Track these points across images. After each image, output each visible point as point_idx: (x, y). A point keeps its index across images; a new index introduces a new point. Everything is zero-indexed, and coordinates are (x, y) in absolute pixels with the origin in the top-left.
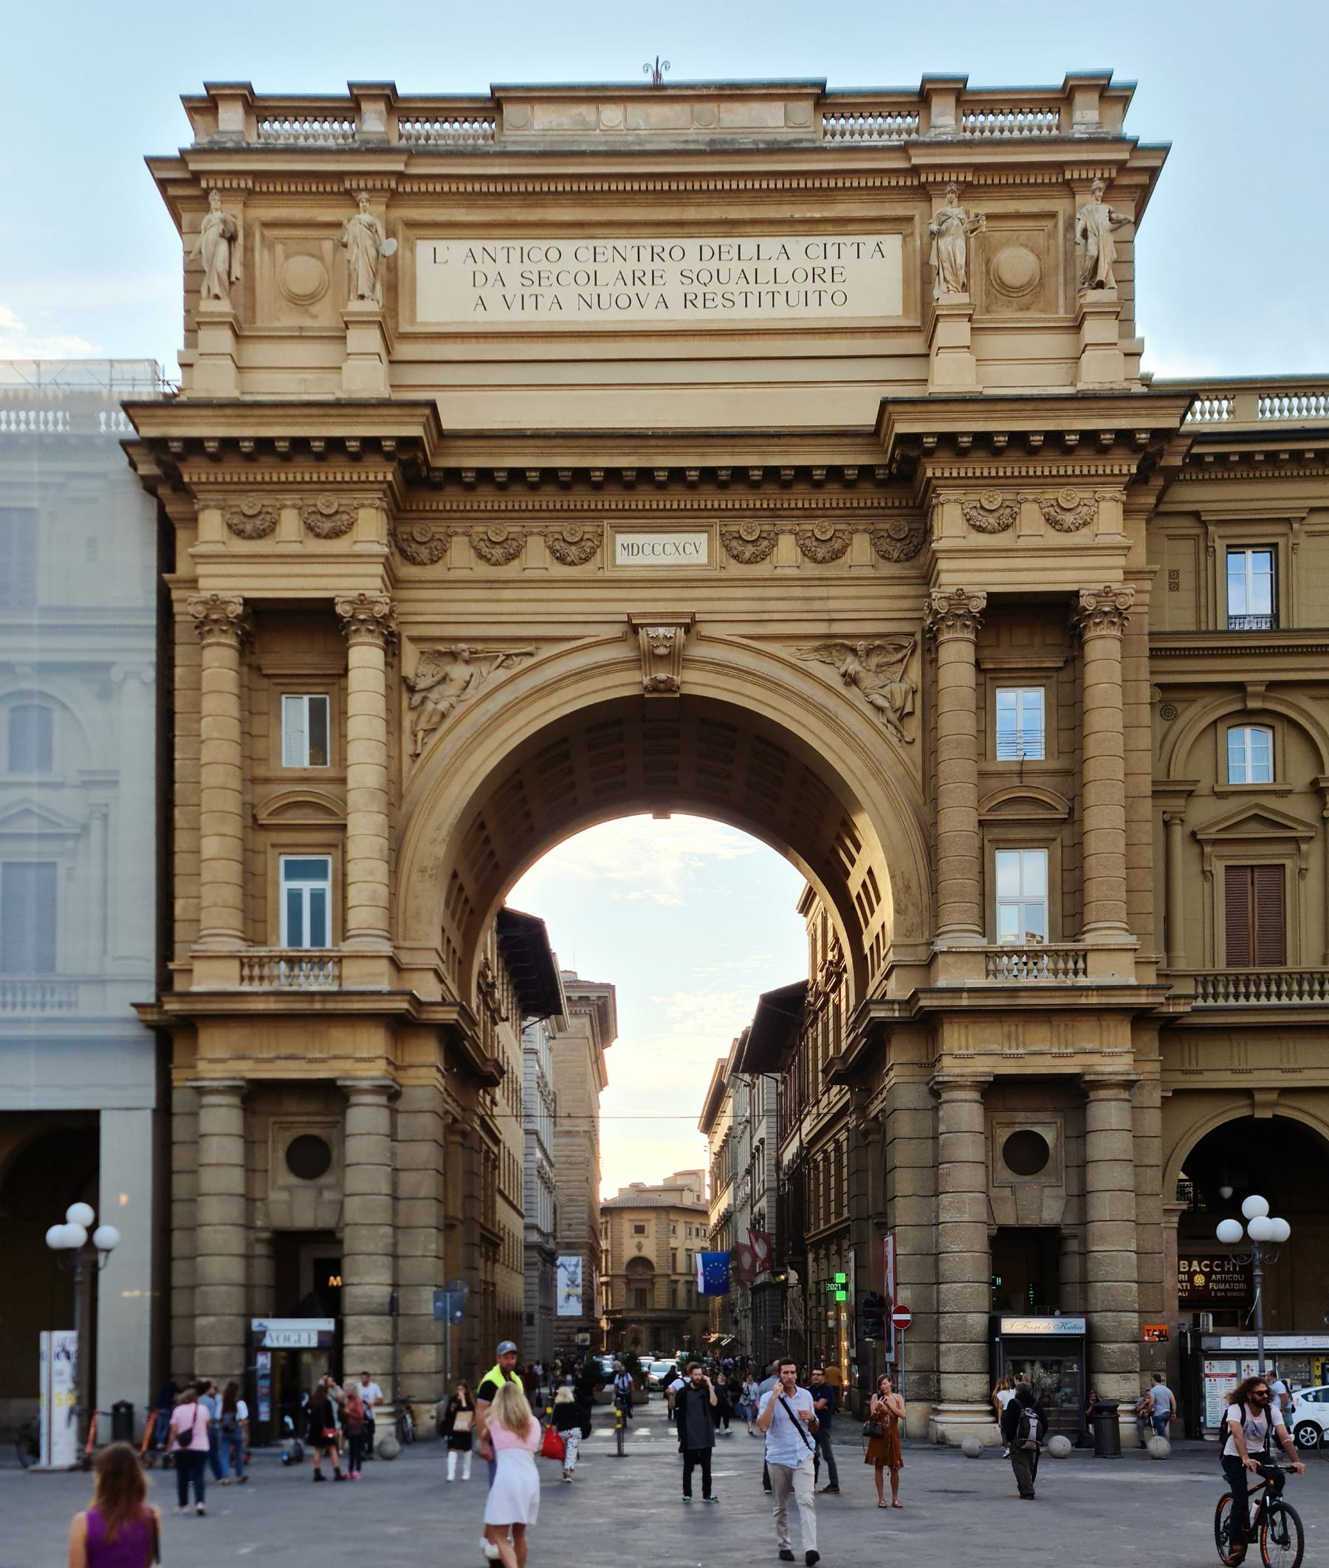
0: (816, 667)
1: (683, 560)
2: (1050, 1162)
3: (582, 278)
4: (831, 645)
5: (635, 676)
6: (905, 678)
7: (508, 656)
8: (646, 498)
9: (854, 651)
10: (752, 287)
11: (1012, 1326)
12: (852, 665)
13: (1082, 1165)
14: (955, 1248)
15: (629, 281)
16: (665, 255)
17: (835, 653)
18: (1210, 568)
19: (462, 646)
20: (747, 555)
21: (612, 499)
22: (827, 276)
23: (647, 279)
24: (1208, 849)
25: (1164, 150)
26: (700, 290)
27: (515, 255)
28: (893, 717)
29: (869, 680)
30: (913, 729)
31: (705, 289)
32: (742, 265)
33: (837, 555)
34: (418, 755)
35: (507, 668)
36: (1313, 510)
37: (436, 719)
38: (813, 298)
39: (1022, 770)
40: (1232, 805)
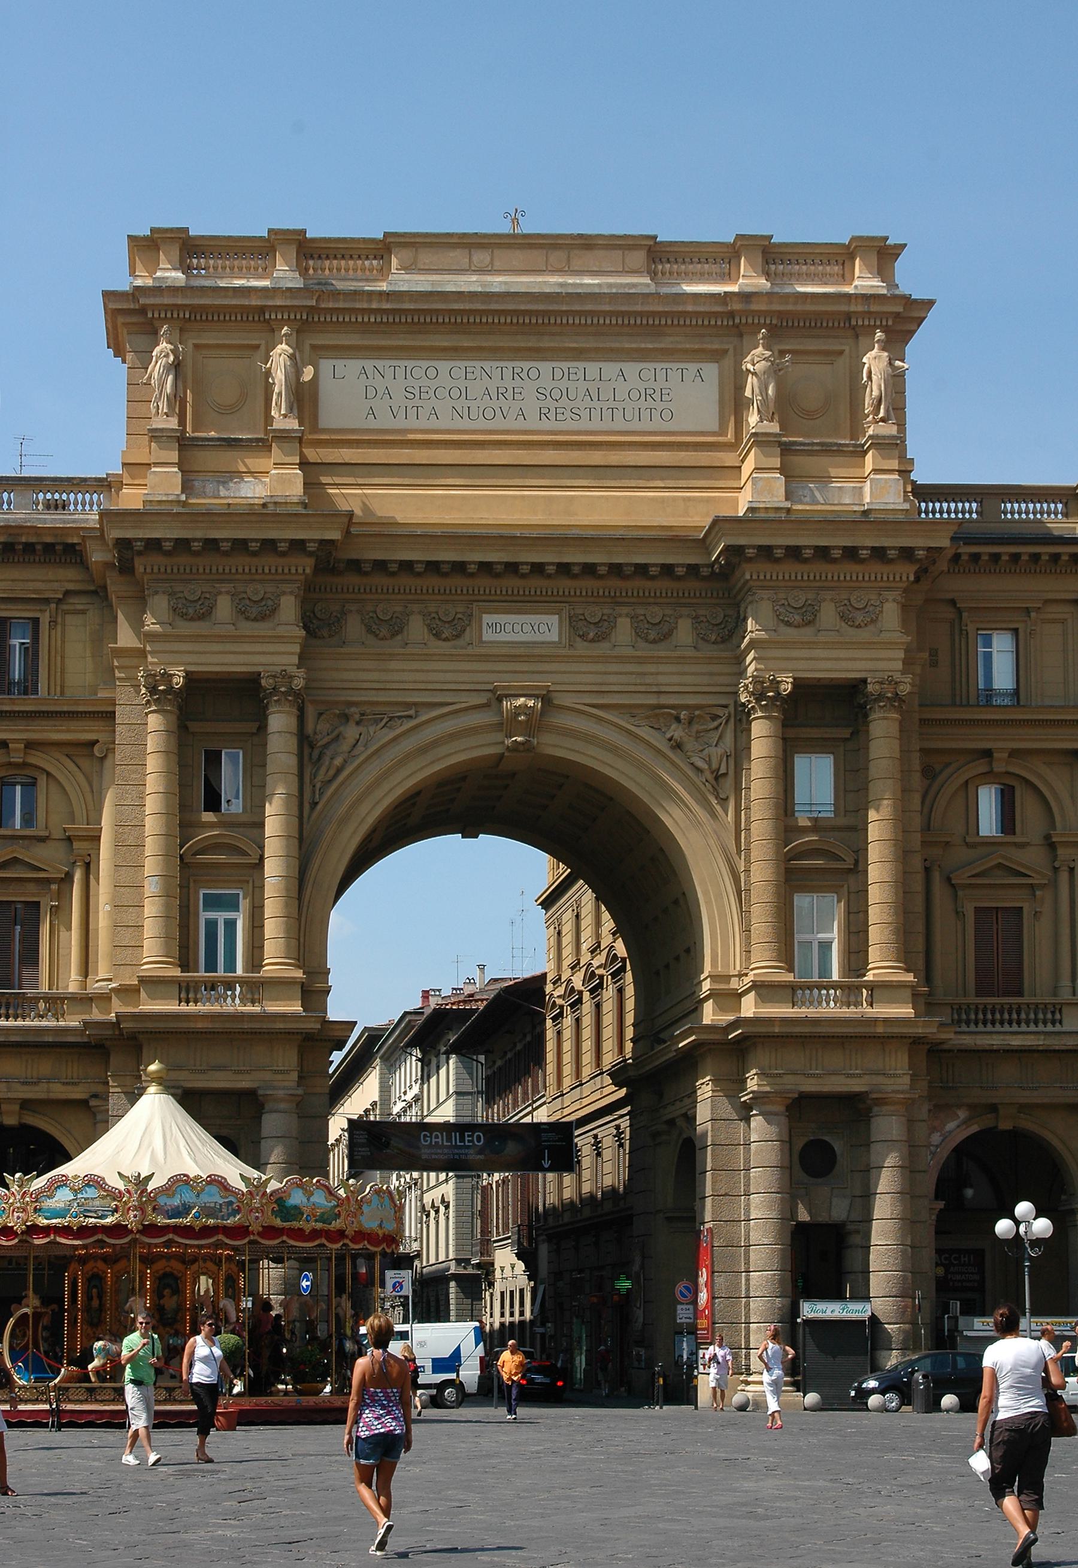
0: (645, 732)
3: (455, 393)
4: (659, 715)
5: (499, 737)
6: (721, 744)
7: (391, 719)
10: (595, 404)
11: (812, 1310)
12: (677, 732)
15: (494, 397)
16: (524, 375)
17: (662, 720)
18: (963, 647)
19: (353, 709)
20: (591, 635)
22: (657, 396)
23: (509, 395)
26: (553, 405)
27: (400, 372)
31: (557, 405)
32: (586, 385)
33: (667, 636)
34: (317, 803)
35: (390, 728)
37: (332, 772)
39: (817, 826)
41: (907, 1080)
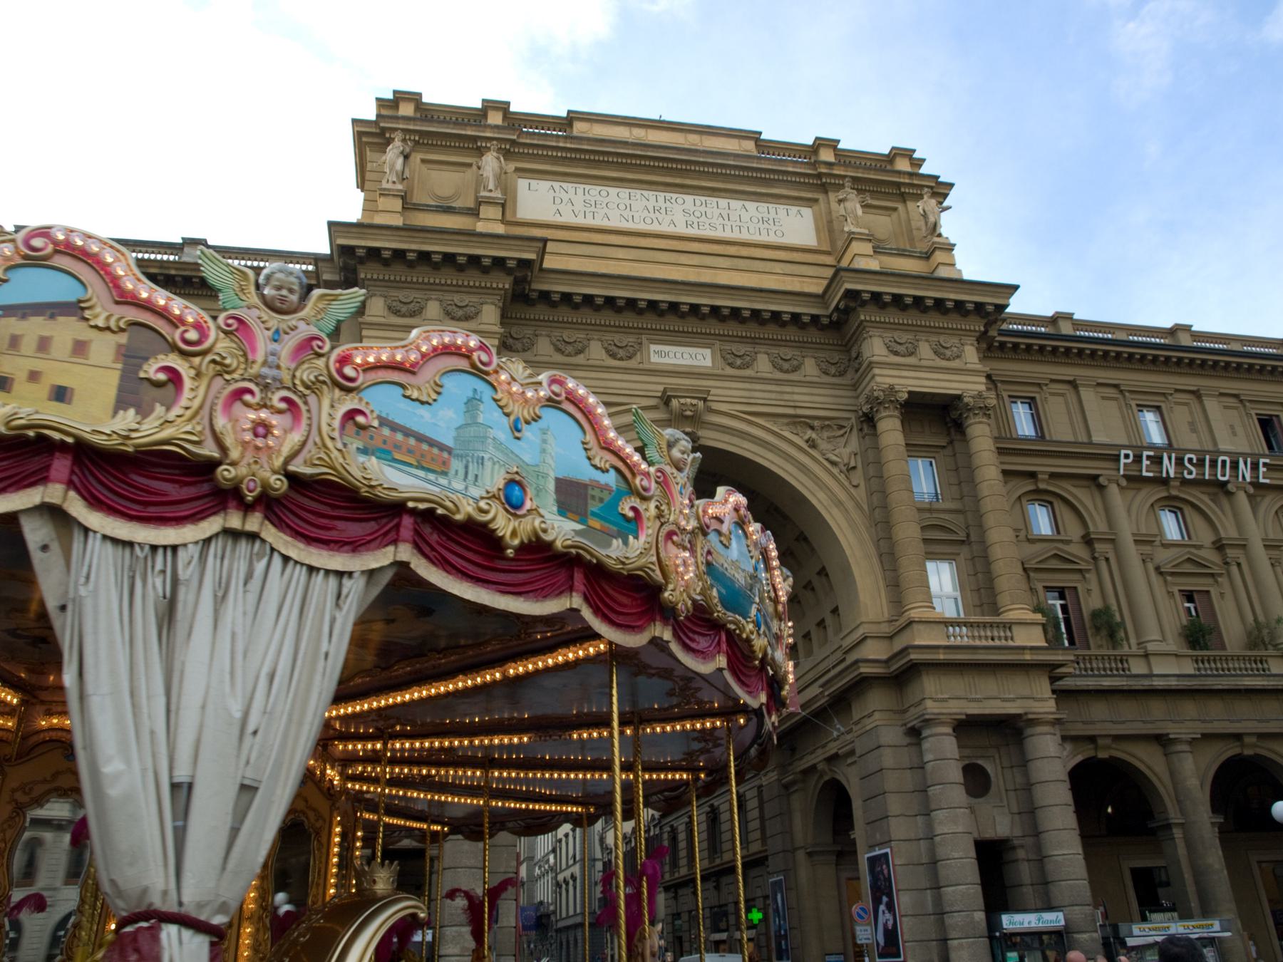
1: (695, 363)
2: (993, 788)
8: (672, 323)
9: (812, 428)
10: (726, 222)
11: (1013, 922)
13: (1028, 787)
14: (956, 855)
15: (651, 210)
21: (650, 321)
22: (771, 222)
23: (663, 211)
24: (1032, 574)
25: (951, 185)
26: (696, 221)
27: (580, 191)
28: (844, 469)
29: (823, 445)
30: (857, 477)
33: (795, 369)
36: (1052, 381)
38: (764, 232)
40: (1039, 546)
41: (1052, 703)
